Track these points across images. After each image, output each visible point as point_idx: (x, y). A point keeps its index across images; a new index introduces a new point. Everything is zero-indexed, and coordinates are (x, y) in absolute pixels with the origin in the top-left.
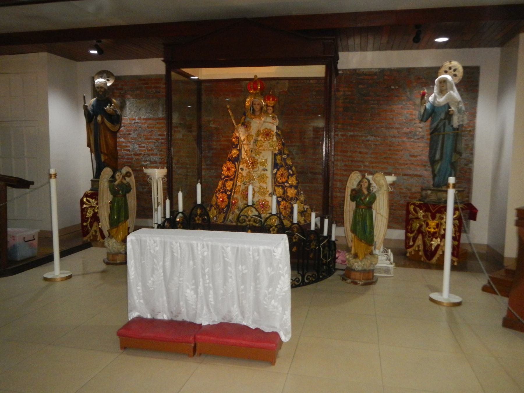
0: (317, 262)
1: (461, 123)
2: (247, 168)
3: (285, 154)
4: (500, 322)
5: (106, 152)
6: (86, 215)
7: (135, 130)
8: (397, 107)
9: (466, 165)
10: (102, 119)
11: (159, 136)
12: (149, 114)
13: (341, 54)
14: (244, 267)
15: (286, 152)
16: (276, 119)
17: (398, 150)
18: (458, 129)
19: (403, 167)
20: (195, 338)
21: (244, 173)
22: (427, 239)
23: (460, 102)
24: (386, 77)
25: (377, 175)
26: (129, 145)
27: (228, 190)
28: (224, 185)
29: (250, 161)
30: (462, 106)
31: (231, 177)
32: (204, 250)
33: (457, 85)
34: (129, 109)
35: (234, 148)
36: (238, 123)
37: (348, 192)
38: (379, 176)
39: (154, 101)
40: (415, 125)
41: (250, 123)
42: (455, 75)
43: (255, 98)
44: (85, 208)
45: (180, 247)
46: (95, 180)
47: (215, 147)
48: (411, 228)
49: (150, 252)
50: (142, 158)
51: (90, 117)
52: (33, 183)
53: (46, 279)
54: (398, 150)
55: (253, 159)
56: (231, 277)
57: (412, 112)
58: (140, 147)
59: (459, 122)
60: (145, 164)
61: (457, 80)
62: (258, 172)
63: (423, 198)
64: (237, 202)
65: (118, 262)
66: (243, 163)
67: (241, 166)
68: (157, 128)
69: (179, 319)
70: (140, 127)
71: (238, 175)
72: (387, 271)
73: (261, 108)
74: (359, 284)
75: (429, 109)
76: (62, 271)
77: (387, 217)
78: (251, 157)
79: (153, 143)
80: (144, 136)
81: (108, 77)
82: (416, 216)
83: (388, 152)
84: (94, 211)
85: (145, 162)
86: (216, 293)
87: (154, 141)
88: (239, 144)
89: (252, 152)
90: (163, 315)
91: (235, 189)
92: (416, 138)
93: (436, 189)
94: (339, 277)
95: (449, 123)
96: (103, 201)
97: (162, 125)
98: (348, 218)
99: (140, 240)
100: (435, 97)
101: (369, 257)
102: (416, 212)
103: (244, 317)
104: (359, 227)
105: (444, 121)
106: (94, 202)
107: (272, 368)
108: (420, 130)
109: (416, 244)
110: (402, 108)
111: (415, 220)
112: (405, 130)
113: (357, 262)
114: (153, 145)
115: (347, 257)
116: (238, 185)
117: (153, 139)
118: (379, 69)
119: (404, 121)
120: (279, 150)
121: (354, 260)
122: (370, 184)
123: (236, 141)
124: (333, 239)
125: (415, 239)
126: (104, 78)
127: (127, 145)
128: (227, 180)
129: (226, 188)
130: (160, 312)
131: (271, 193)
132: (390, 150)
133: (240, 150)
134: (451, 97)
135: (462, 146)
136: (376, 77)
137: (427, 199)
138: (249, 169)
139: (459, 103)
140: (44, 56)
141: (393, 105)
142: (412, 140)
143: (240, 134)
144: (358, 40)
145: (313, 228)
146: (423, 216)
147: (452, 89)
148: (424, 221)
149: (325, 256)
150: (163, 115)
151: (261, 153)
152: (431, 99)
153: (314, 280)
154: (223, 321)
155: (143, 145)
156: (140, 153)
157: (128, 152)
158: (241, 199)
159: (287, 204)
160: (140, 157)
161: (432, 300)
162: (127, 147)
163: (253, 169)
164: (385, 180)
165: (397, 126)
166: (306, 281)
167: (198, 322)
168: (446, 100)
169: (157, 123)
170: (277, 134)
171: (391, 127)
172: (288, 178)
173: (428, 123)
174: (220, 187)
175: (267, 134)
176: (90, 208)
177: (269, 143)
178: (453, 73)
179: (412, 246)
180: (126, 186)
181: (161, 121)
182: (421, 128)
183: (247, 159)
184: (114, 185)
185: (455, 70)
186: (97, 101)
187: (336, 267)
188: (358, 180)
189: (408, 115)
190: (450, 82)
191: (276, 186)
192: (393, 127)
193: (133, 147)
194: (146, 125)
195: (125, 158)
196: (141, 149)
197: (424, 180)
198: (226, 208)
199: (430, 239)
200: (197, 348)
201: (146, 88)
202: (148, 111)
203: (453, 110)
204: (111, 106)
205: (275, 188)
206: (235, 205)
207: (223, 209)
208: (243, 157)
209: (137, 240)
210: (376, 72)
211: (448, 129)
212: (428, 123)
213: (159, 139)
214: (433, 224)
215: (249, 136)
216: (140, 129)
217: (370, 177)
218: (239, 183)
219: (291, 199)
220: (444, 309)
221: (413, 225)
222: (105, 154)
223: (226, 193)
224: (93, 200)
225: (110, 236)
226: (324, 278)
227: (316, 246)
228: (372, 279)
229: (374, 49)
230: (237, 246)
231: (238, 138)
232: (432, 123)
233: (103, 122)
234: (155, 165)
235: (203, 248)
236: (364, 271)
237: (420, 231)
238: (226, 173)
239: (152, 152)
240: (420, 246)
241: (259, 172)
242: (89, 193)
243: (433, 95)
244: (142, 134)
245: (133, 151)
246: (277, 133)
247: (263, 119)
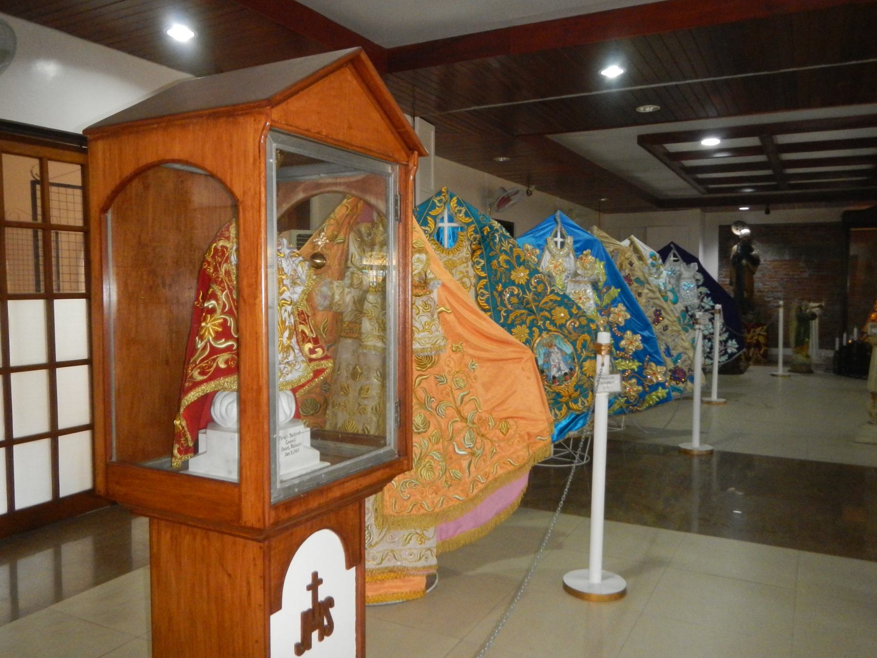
155: (767, 283)
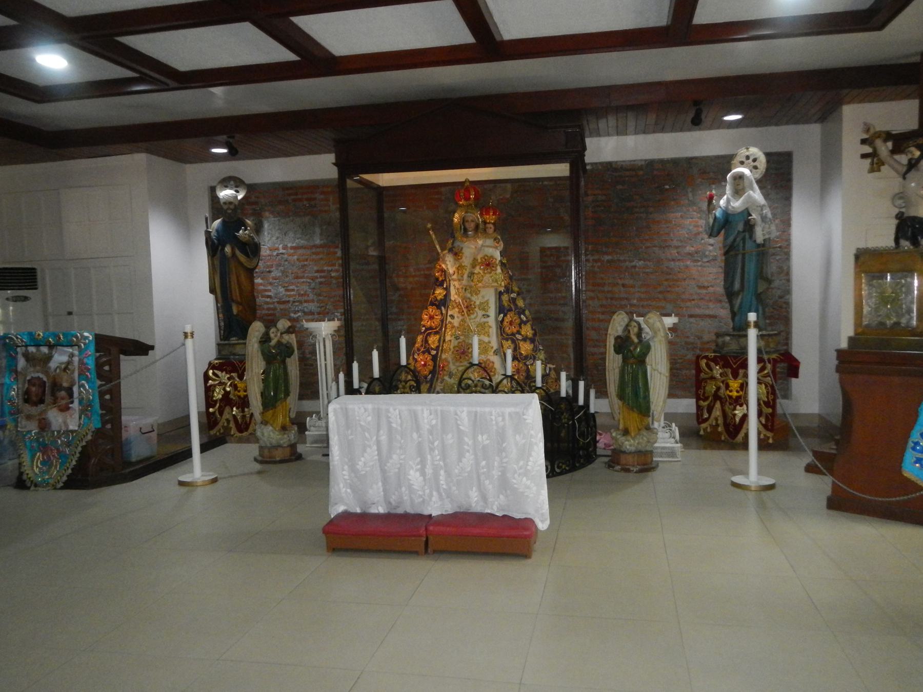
0: (571, 445)
1: (767, 236)
2: (459, 315)
3: (514, 292)
4: (825, 503)
5: (239, 300)
6: (213, 396)
7: (279, 265)
8: (675, 216)
9: (781, 297)
10: (233, 249)
11: (316, 272)
12: (300, 240)
13: (588, 141)
14: (485, 437)
15: (516, 289)
16: (499, 241)
17: (677, 280)
18: (763, 245)
19: (688, 304)
20: (426, 529)
21: (456, 322)
22: (728, 408)
23: (764, 205)
24: (655, 172)
25: (650, 315)
26: (269, 288)
27: (432, 349)
28: (426, 341)
29: (464, 305)
30: (767, 212)
31: (436, 329)
32: (432, 417)
33: (759, 182)
34: (269, 233)
35: (438, 286)
36: (443, 249)
37: (611, 342)
38: (653, 317)
39: (307, 219)
40: (703, 241)
41: (462, 248)
42: (756, 168)
43: (466, 212)
44: (211, 386)
45: (400, 414)
46: (223, 342)
47: (403, 285)
48: (704, 393)
49: (359, 424)
50: (290, 308)
51: (214, 247)
52: (152, 348)
53: (182, 484)
54: (677, 280)
55: (468, 300)
56: (468, 451)
57: (697, 222)
58: (287, 290)
59: (764, 235)
60: (296, 316)
61: (759, 174)
62: (476, 320)
63: (719, 348)
64: (448, 365)
65: (278, 459)
66: (454, 308)
67: (450, 313)
68: (313, 260)
69: (400, 511)
70: (286, 260)
71: (446, 325)
72: (672, 453)
73: (477, 227)
74: (633, 471)
75: (721, 217)
76: (204, 473)
77: (667, 374)
78: (464, 298)
79: (308, 284)
80: (292, 273)
81: (237, 187)
82: (710, 375)
83: (666, 283)
84: (224, 389)
85: (295, 313)
86: (449, 474)
87: (309, 280)
88: (445, 280)
89: (467, 292)
90: (378, 507)
91: (443, 346)
92: (705, 260)
93: (735, 333)
94: (604, 465)
95: (751, 237)
96: (252, 371)
97: (321, 256)
98: (612, 378)
99: (346, 409)
100: (728, 201)
101: (645, 433)
102: (711, 369)
103: (486, 503)
104: (629, 390)
105: (743, 234)
106: (225, 377)
107: (529, 561)
108: (711, 248)
109: (713, 416)
110: (681, 217)
111: (708, 381)
112: (689, 249)
113: (628, 441)
114: (307, 287)
115: (614, 434)
116: (446, 341)
117: (307, 277)
118: (646, 160)
119: (686, 235)
120: (505, 287)
121: (623, 438)
122: (640, 329)
123: (441, 275)
124: (592, 410)
125: (710, 409)
126: (231, 189)
127: (267, 288)
128: (429, 334)
129: (429, 345)
130: (374, 504)
131: (497, 349)
132: (667, 280)
133: (447, 289)
134: (750, 199)
135: (772, 268)
136: (641, 173)
137: (725, 349)
138: (463, 315)
139: (762, 207)
140: (140, 159)
141: (669, 212)
142: (699, 264)
143: (447, 265)
144: (612, 121)
145: (563, 394)
146: (721, 374)
147: (752, 189)
148: (723, 382)
149: (582, 435)
150: (321, 240)
151: (479, 291)
152: (722, 202)
153: (567, 468)
154: (458, 510)
155: (291, 287)
156: (287, 299)
157: (268, 300)
158: (453, 360)
159: (521, 365)
160: (287, 307)
161: (735, 485)
162: (266, 291)
163: (468, 315)
164: (661, 322)
165: (675, 243)
166: (558, 470)
167: (426, 513)
168: (743, 203)
169: (313, 253)
170: (503, 265)
171: (667, 246)
172: (521, 328)
173: (721, 238)
174: (420, 345)
175: (488, 264)
176: (219, 386)
177: (491, 277)
178: (753, 164)
179: (707, 420)
180: (287, 347)
181: (318, 250)
182: (712, 245)
183: (459, 302)
184: (270, 346)
185: (755, 160)
186: (224, 222)
187: (598, 453)
188: (624, 324)
189: (691, 228)
190: (747, 177)
191: (503, 339)
192: (670, 246)
193: (276, 291)
194: (295, 257)
195: (264, 309)
196: (289, 293)
197: (721, 322)
198: (430, 375)
199: (732, 407)
200: (429, 543)
201: (294, 200)
202: (298, 236)
203: (754, 219)
204: (246, 229)
205: (502, 343)
206: (445, 370)
207: (426, 377)
208: (453, 299)
209: (342, 408)
210: (642, 165)
211: (749, 244)
212: (721, 238)
213: (317, 278)
214: (736, 385)
215: (460, 268)
216: (286, 263)
217: (641, 319)
218: (448, 338)
219: (526, 357)
220: (751, 496)
221: (707, 388)
222: (238, 303)
223: (429, 353)
224: (224, 373)
225: (265, 423)
226: (583, 466)
227: (569, 420)
228: (651, 463)
229: (636, 133)
230: (474, 409)
231: (444, 271)
232: (726, 239)
233: (234, 254)
234: (322, 315)
235: (431, 414)
236: (639, 453)
237: (716, 397)
238: (429, 323)
239: (306, 298)
240: (719, 418)
241: (478, 319)
242: (217, 363)
243: (725, 197)
244: (290, 271)
245: (276, 298)
246: (501, 261)
247: (480, 242)
